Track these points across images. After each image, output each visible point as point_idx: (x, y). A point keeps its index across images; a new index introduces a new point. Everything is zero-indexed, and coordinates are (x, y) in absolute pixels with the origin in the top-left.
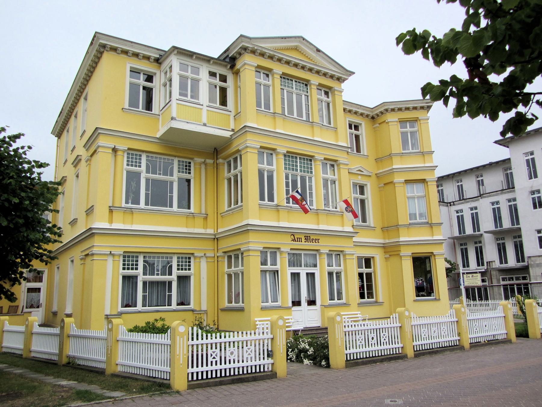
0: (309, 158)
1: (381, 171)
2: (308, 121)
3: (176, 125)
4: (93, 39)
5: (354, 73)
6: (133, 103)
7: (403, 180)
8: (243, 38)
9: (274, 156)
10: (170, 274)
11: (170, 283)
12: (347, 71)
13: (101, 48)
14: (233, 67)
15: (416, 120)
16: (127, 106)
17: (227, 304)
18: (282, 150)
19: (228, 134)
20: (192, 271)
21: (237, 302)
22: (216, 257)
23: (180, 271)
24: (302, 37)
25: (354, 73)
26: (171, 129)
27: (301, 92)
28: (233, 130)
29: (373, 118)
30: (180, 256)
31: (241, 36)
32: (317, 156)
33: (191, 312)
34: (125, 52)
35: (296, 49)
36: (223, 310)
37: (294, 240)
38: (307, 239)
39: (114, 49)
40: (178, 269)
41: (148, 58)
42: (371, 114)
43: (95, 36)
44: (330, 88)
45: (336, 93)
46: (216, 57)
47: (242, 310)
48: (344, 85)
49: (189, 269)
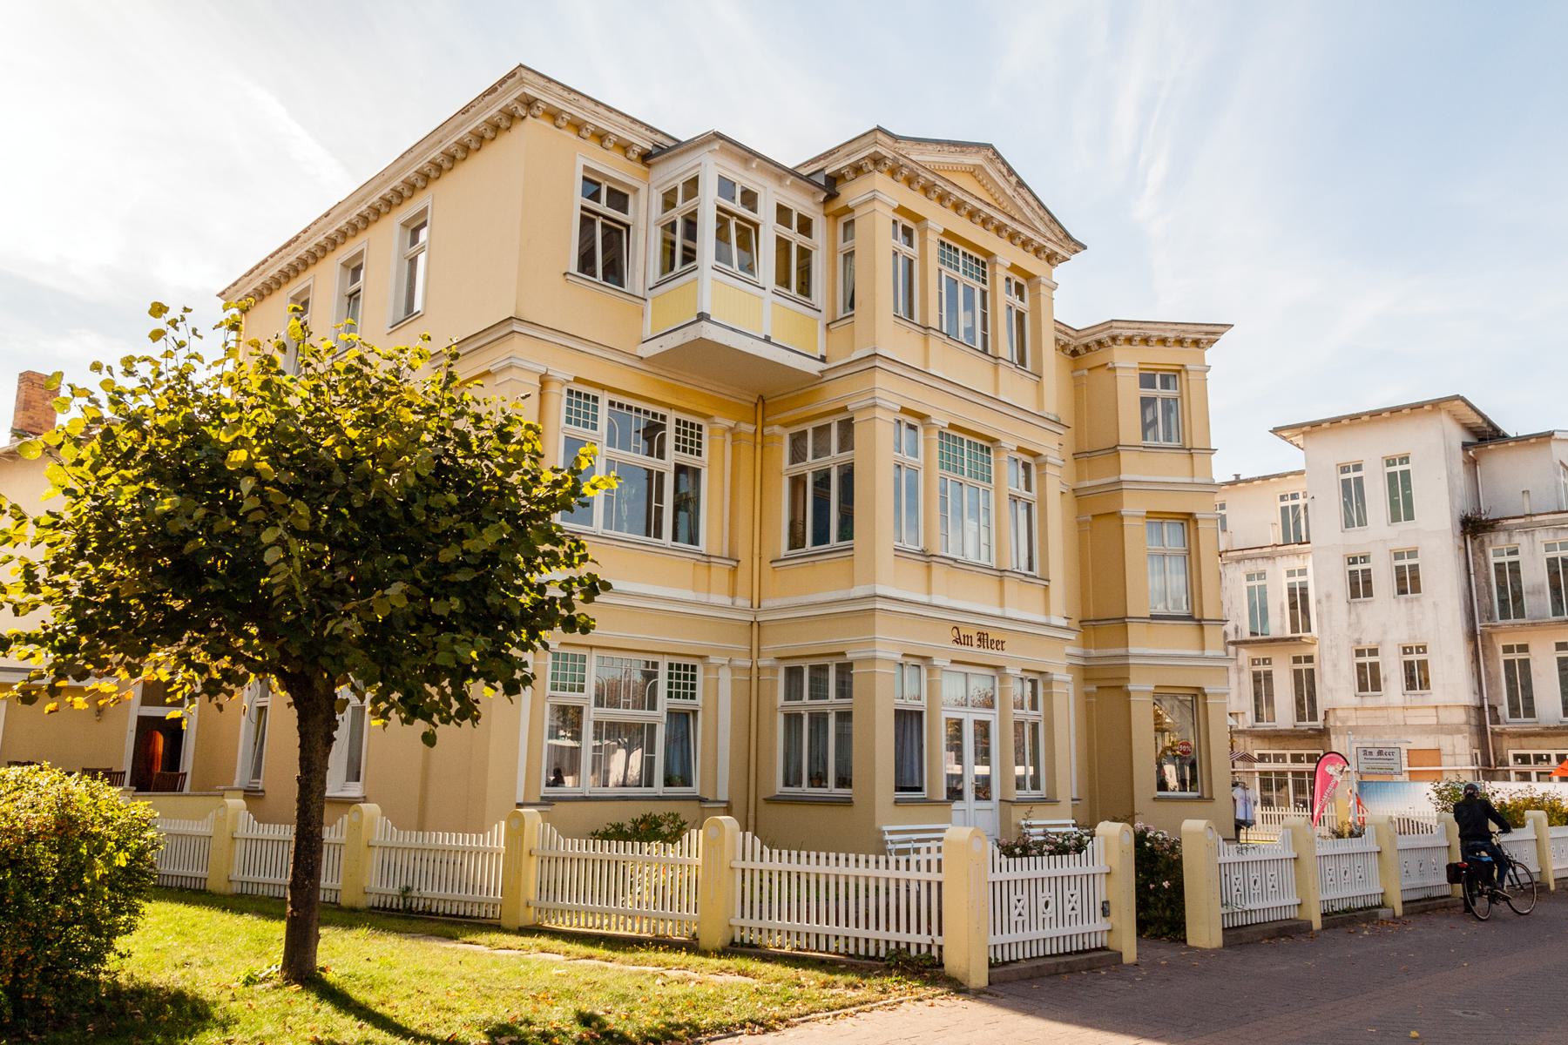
0: (986, 444)
1: (1088, 484)
2: (985, 351)
3: (709, 332)
4: (503, 81)
5: (1085, 248)
6: (586, 263)
7: (1142, 511)
8: (880, 136)
9: (921, 430)
10: (653, 706)
11: (652, 727)
12: (1068, 236)
13: (516, 105)
14: (832, 196)
15: (1180, 371)
16: (574, 268)
17: (779, 788)
18: (940, 421)
19: (814, 368)
20: (699, 700)
21: (818, 779)
22: (755, 670)
23: (674, 700)
24: (989, 147)
25: (1085, 248)
26: (701, 341)
27: (974, 281)
28: (823, 359)
29: (1075, 353)
30: (676, 660)
31: (879, 129)
32: (1009, 444)
33: (696, 804)
34: (578, 126)
35: (974, 172)
36: (770, 801)
37: (958, 641)
38: (983, 639)
39: (553, 115)
40: (670, 695)
41: (625, 147)
42: (1073, 343)
43: (512, 75)
44: (1029, 277)
45: (1042, 288)
46: (790, 166)
47: (848, 802)
48: (1059, 273)
49: (693, 696)
